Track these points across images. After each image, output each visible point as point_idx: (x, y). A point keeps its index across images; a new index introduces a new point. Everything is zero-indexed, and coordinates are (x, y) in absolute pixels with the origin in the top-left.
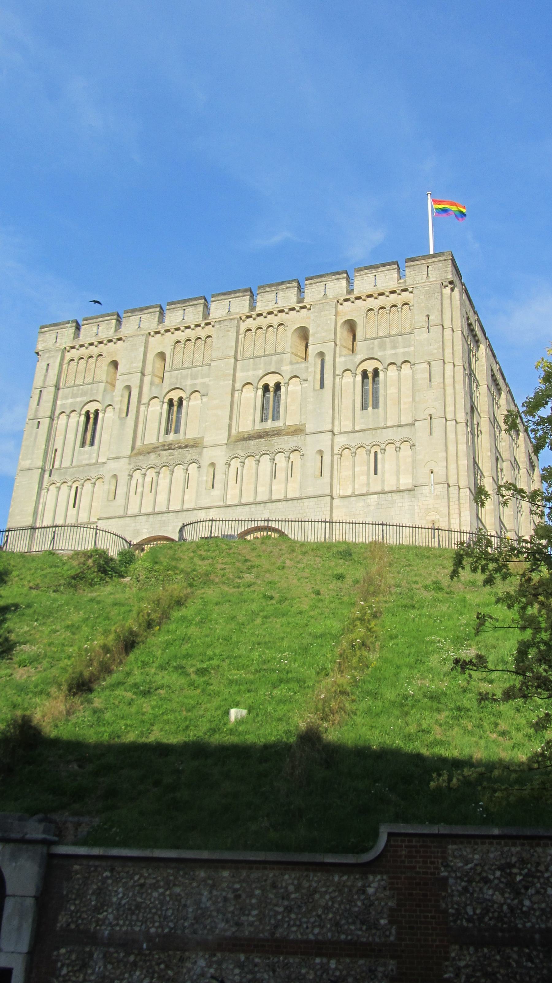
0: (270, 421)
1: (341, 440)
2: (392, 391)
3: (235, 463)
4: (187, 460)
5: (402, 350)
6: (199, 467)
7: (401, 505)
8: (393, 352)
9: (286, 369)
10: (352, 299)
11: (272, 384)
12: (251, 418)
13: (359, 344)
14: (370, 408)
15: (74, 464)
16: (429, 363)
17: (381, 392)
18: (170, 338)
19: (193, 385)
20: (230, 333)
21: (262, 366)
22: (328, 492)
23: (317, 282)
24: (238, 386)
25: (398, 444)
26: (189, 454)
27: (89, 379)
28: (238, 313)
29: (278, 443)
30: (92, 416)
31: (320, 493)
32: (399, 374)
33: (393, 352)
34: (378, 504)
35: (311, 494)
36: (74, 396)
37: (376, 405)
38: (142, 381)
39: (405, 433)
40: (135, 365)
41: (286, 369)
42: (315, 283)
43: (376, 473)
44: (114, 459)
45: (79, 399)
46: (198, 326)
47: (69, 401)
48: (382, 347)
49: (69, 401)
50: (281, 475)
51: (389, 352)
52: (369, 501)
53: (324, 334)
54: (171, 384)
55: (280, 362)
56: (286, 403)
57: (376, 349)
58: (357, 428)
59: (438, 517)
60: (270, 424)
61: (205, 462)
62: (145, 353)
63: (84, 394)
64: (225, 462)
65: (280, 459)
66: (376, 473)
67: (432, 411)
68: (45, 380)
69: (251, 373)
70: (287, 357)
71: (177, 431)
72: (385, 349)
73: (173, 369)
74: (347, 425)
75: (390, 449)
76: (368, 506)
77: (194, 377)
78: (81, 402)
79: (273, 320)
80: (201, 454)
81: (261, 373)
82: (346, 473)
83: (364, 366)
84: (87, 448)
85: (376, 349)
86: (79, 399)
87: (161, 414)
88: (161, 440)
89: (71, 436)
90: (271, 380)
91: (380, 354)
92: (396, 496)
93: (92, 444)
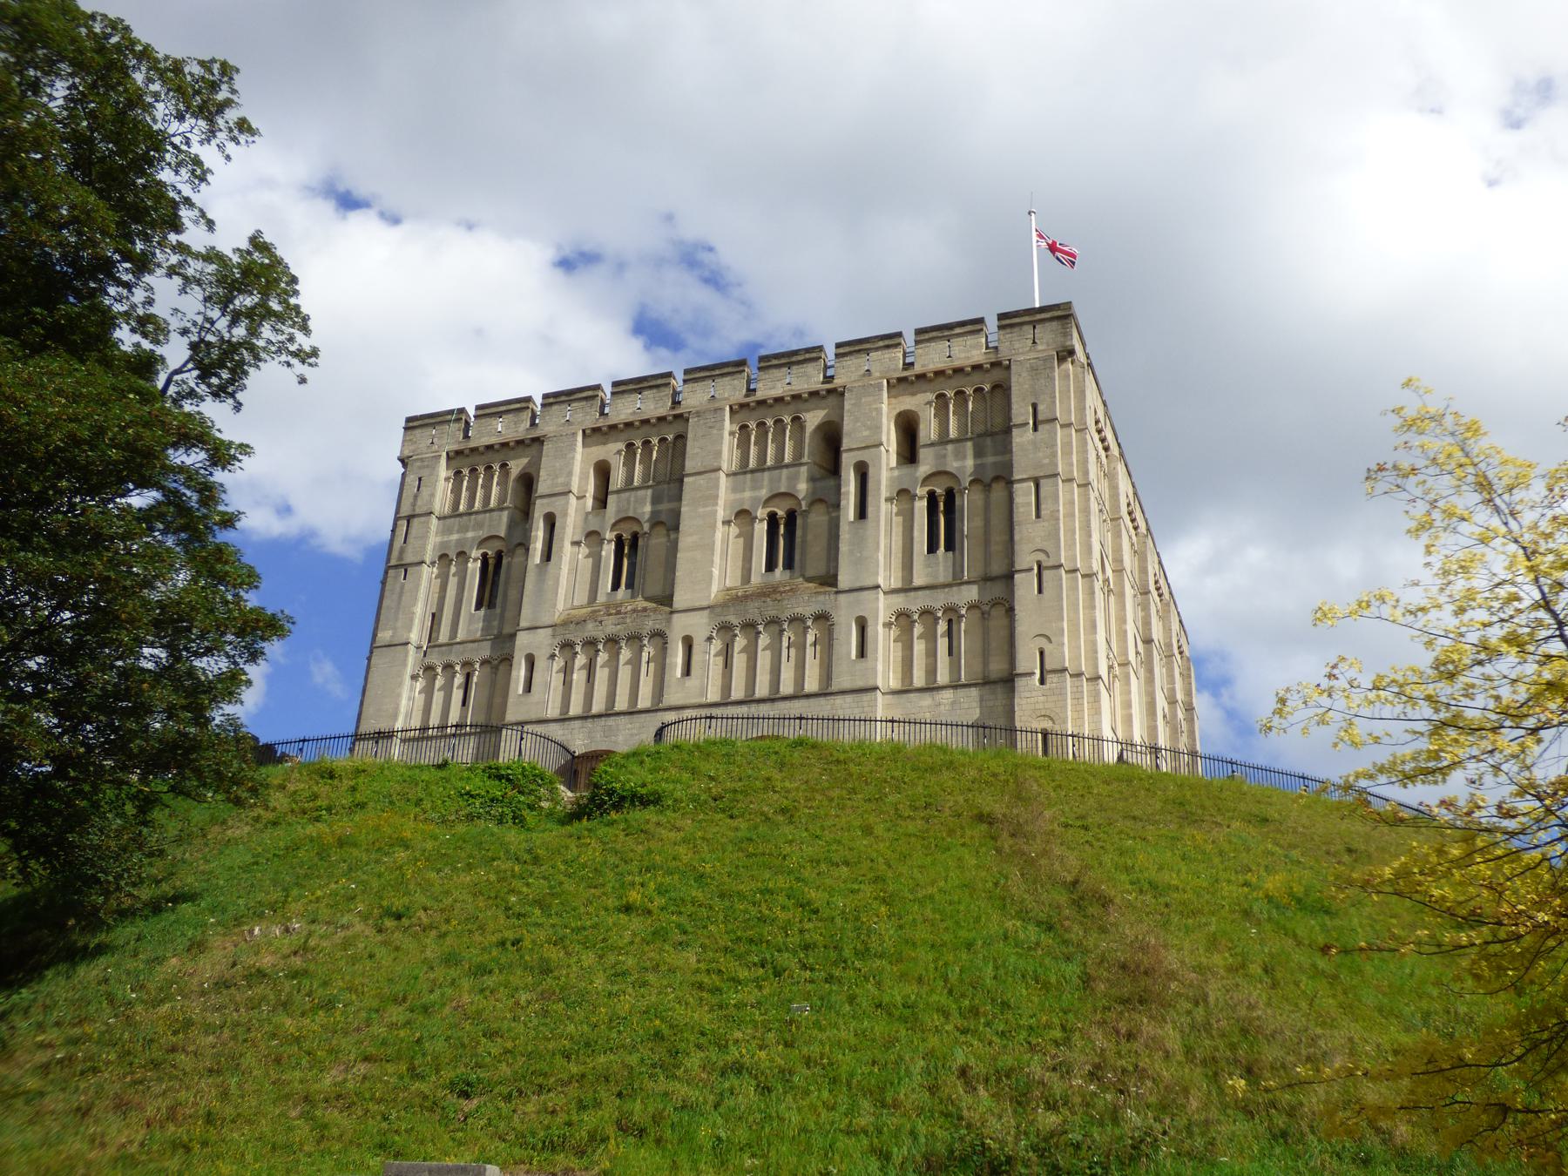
11: (781, 513)
15: (460, 637)
21: (766, 482)
30: (491, 562)
35: (847, 685)
47: (455, 537)
53: (866, 433)
56: (804, 541)
58: (917, 582)
63: (479, 526)
67: (1041, 557)
68: (414, 505)
69: (747, 494)
80: (669, 621)
81: (764, 493)
85: (950, 457)
86: (470, 534)
91: (955, 464)
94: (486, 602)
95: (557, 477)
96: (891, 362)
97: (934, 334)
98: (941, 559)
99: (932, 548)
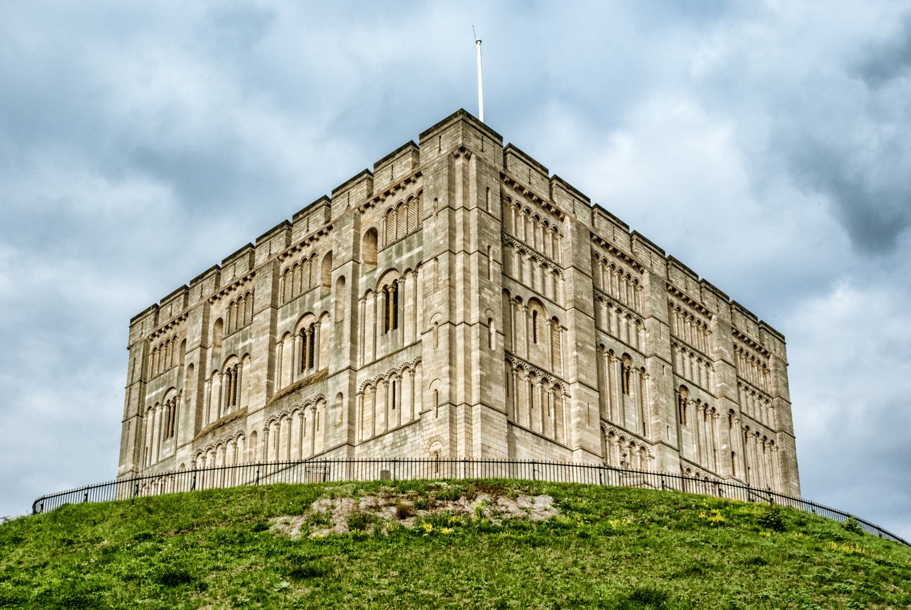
0: (305, 371)
1: (362, 376)
2: (409, 303)
3: (272, 427)
4: (235, 433)
5: (416, 250)
6: (244, 439)
7: (412, 439)
8: (409, 254)
9: (318, 305)
10: (371, 203)
12: (289, 372)
13: (381, 257)
14: (389, 332)
16: (436, 259)
17: (400, 307)
18: (226, 300)
19: (244, 348)
20: (268, 279)
21: (298, 308)
22: (345, 440)
23: (342, 193)
24: (278, 337)
25: (412, 367)
26: (237, 427)
27: (168, 366)
28: (276, 253)
29: (309, 394)
30: (171, 405)
31: (339, 443)
32: (416, 281)
33: (409, 254)
34: (392, 444)
35: (332, 445)
36: (157, 387)
37: (395, 327)
38: (203, 357)
39: (417, 351)
40: (196, 339)
41: (318, 305)
42: (340, 195)
43: (394, 407)
44: (182, 446)
45: (160, 390)
46: (245, 279)
47: (154, 393)
48: (399, 253)
49: (154, 393)
50: (309, 430)
51: (406, 256)
52: (385, 442)
53: (344, 254)
54: (227, 353)
55: (312, 300)
57: (394, 256)
59: (440, 446)
60: (306, 374)
61: (248, 433)
62: (205, 324)
64: (264, 427)
65: (308, 412)
66: (394, 407)
69: (289, 320)
70: (318, 291)
71: (234, 404)
72: (402, 255)
73: (229, 333)
74: (369, 357)
75: (406, 375)
76: (384, 448)
77: (244, 339)
78: (162, 392)
79: (306, 252)
80: (245, 423)
81: (296, 317)
82: (368, 414)
83: (384, 282)
84: (168, 441)
86: (160, 390)
87: (221, 387)
88: (222, 416)
89: (156, 431)
90: (306, 323)
91: (397, 261)
92: (408, 431)
93: (172, 436)
94: (170, 434)
95: (194, 338)
96: (359, 194)
97: (384, 164)
98: (390, 337)
99: (387, 329)
